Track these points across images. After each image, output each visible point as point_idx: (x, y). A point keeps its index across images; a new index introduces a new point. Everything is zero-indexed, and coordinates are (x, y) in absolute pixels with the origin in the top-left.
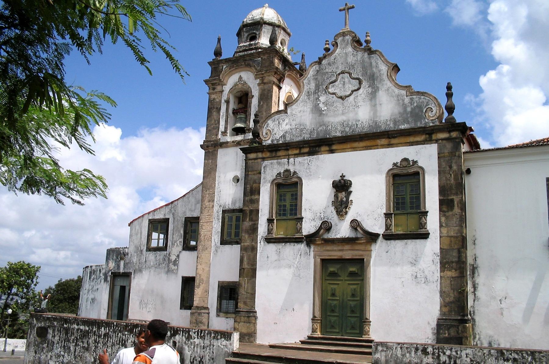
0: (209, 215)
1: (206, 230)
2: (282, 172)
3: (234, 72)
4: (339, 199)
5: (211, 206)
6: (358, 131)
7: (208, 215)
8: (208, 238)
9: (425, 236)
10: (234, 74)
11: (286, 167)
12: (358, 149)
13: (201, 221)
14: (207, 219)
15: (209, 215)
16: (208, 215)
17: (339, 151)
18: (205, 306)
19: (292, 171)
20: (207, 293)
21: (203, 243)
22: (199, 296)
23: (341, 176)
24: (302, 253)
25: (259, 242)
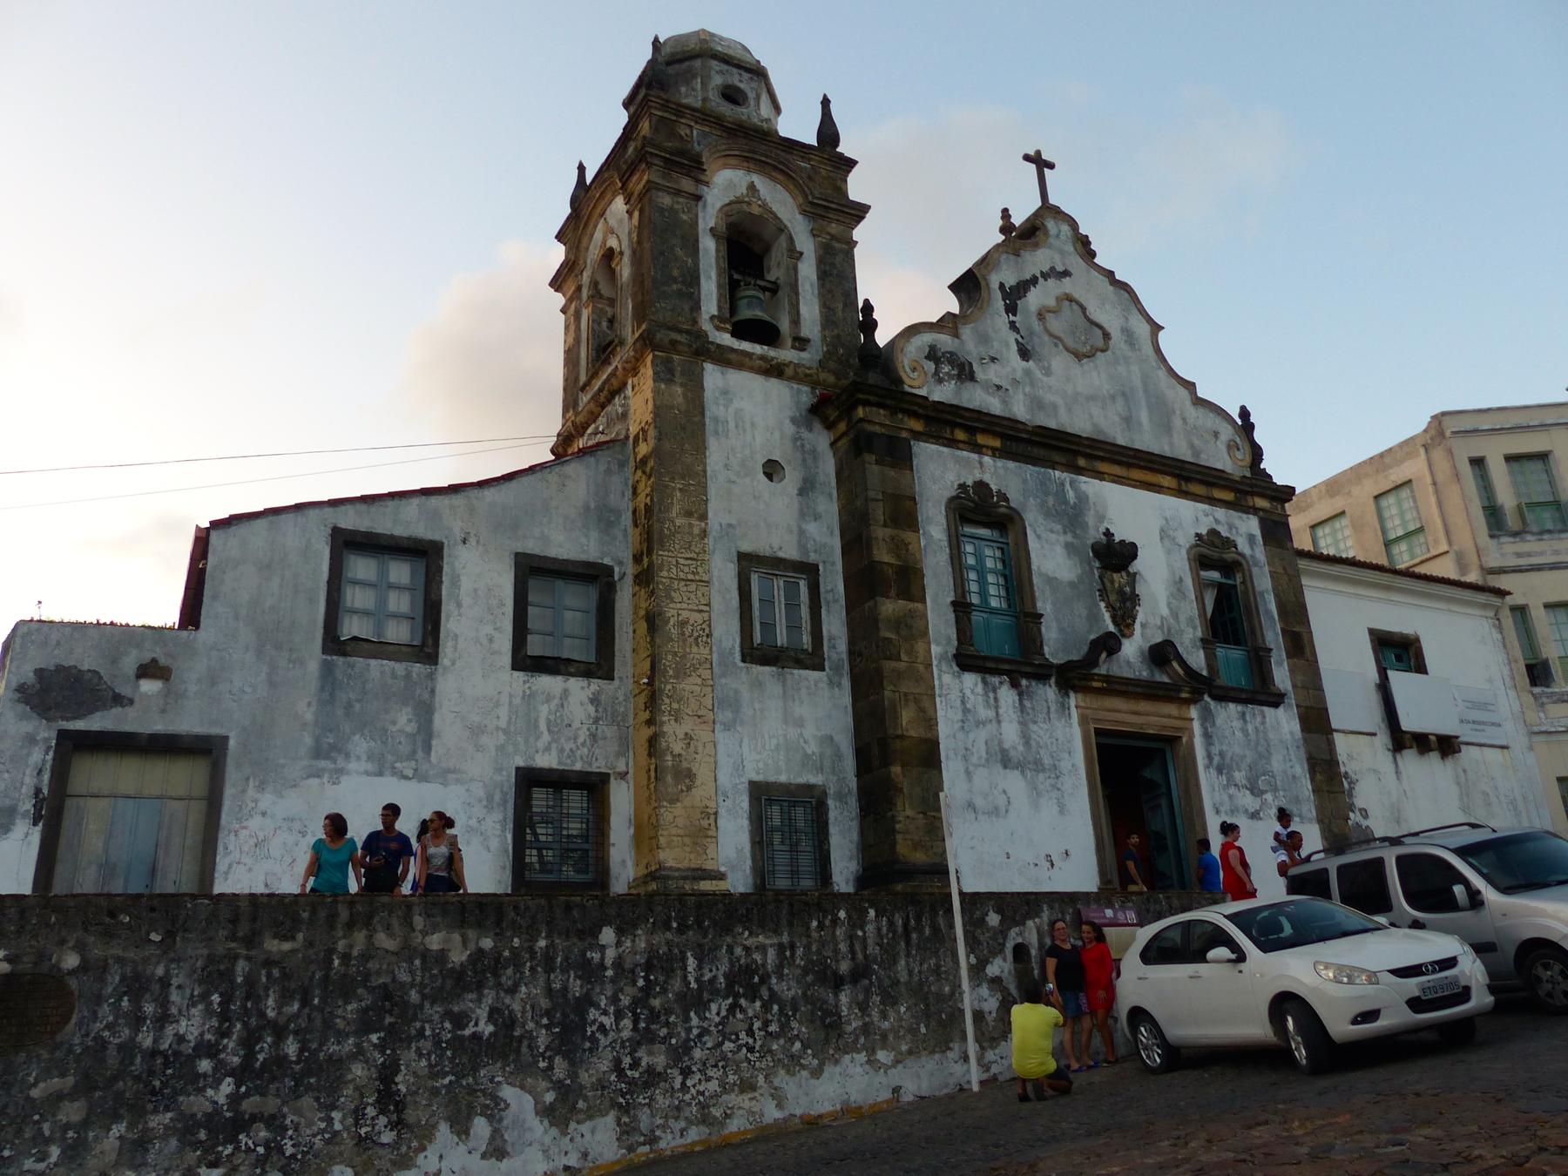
0: (691, 559)
1: (684, 606)
2: (970, 483)
3: (733, 161)
4: (1117, 585)
5: (696, 531)
6: (1108, 440)
7: (687, 559)
8: (696, 634)
9: (1276, 700)
10: (734, 167)
11: (978, 476)
12: (1128, 482)
13: (664, 574)
14: (686, 570)
15: (691, 559)
16: (687, 559)
17: (1090, 473)
18: (709, 865)
19: (994, 488)
20: (712, 817)
21: (675, 646)
22: (680, 832)
23: (1104, 534)
24: (1053, 708)
25: (935, 663)
